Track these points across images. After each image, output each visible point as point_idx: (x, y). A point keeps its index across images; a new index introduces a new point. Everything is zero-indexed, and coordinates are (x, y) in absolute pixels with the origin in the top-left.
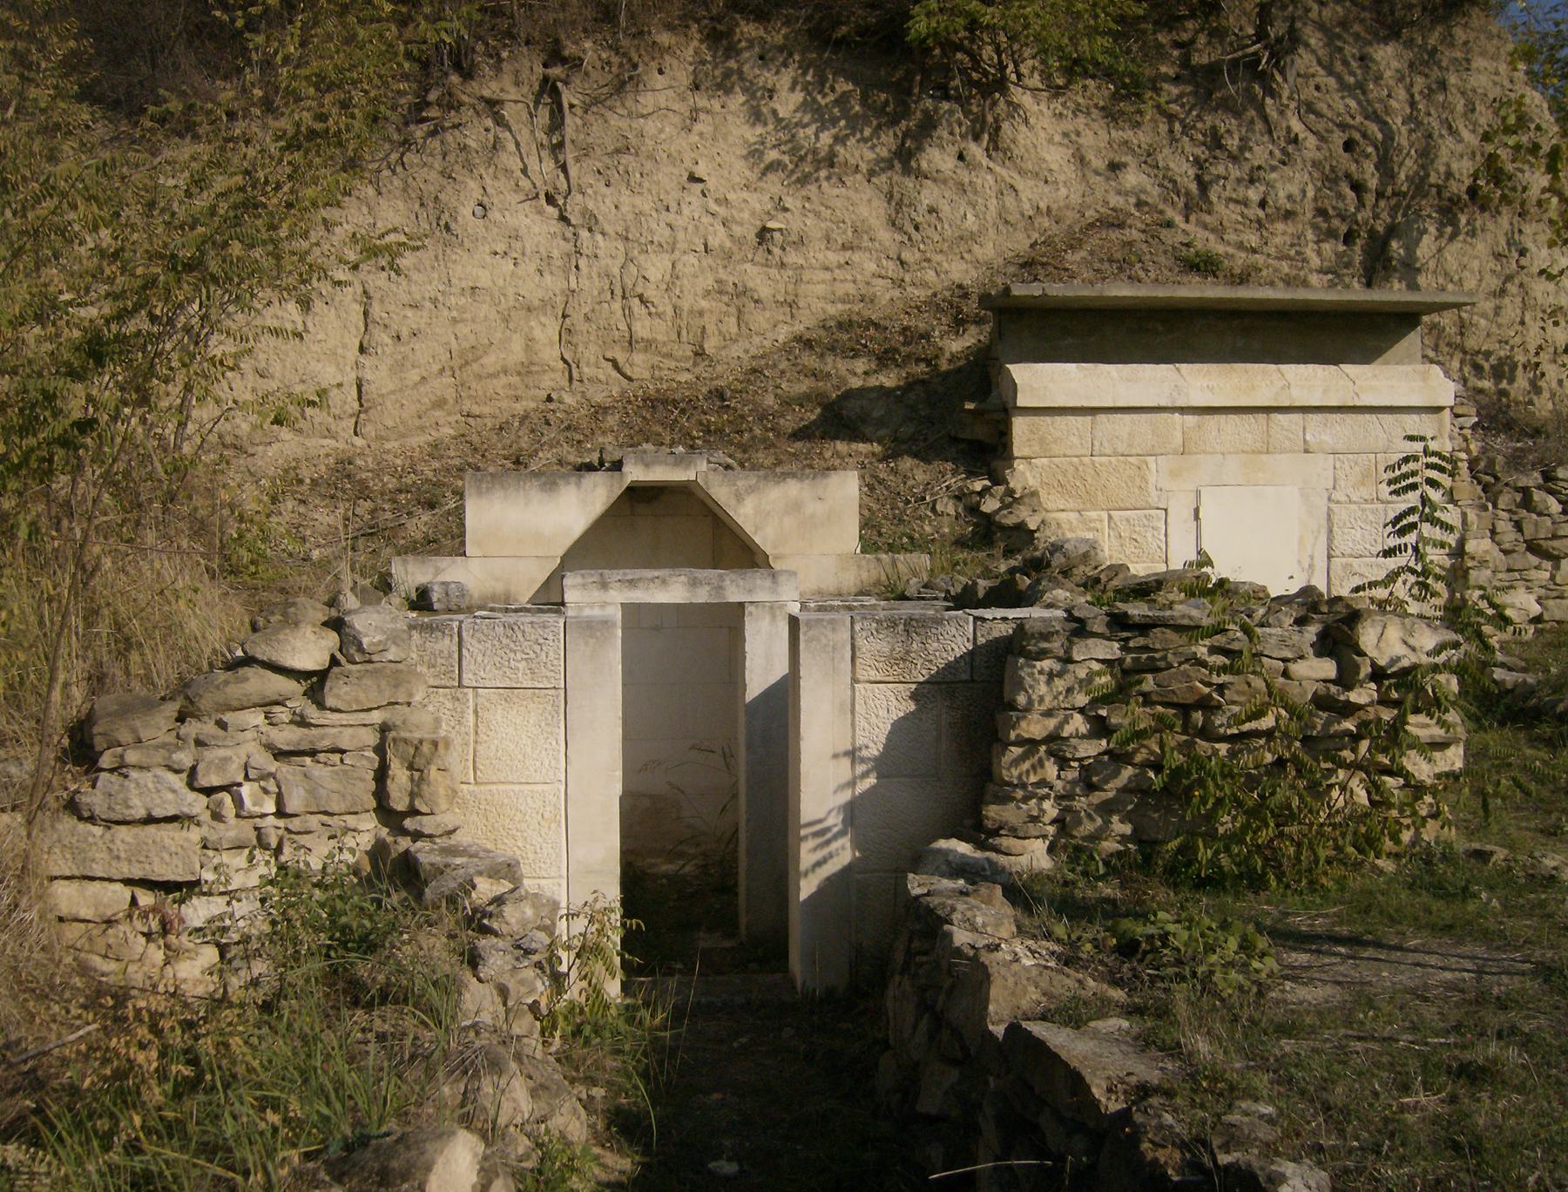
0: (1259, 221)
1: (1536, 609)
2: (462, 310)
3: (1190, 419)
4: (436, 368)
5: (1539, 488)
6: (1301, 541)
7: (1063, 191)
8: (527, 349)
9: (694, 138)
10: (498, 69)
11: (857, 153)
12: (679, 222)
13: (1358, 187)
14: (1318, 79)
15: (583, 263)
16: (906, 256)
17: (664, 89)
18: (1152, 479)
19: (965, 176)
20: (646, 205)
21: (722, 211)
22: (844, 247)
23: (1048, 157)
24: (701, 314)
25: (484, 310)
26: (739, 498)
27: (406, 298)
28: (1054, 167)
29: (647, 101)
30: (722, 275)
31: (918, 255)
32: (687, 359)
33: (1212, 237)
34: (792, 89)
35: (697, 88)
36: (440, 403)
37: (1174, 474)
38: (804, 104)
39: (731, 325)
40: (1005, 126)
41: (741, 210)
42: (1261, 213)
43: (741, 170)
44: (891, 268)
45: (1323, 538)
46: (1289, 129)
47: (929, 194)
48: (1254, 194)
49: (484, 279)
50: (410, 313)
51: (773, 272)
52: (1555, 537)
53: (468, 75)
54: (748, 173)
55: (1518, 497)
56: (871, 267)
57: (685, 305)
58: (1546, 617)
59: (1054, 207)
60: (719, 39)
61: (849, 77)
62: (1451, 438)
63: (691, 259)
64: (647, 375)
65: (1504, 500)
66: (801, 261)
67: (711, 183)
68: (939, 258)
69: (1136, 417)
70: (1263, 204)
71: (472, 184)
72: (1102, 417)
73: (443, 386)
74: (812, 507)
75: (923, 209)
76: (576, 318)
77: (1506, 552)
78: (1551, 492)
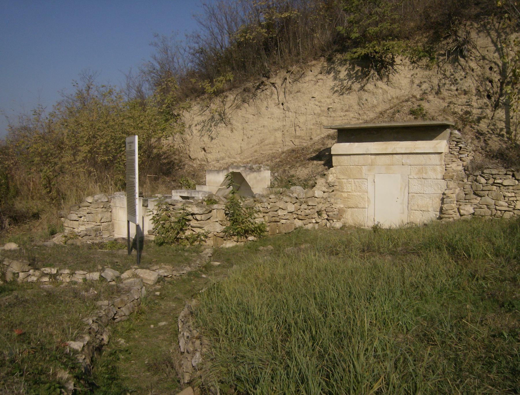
0: (456, 95)
1: (472, 211)
2: (261, 131)
3: (373, 157)
4: (256, 143)
5: (480, 175)
6: (401, 188)
7: (403, 91)
8: (275, 139)
9: (317, 86)
10: (276, 75)
11: (356, 86)
12: (308, 107)
13: (491, 82)
14: (488, 48)
15: (286, 119)
16: (360, 112)
17: (310, 76)
18: (364, 171)
19: (375, 90)
20: (300, 104)
21: (319, 104)
22: (346, 111)
23: (402, 82)
24: (311, 129)
25: (266, 131)
26: (247, 176)
27: (250, 129)
28: (403, 85)
29: (307, 79)
30: (317, 120)
31: (363, 112)
32: (308, 140)
33: (441, 101)
34: (346, 71)
35: (321, 73)
36: (256, 151)
37: (369, 170)
38: (347, 74)
39: (318, 132)
40: (390, 75)
41: (324, 104)
42: (456, 93)
43: (327, 92)
44: (357, 115)
45: (407, 188)
46: (469, 67)
47: (365, 96)
48: (454, 88)
49: (266, 123)
50: (251, 132)
51: (329, 118)
52: (482, 190)
53: (268, 78)
54: (329, 94)
55: (475, 178)
56: (352, 115)
57: (308, 128)
58: (476, 214)
59: (399, 96)
60: (330, 60)
61: (358, 65)
62: (444, 161)
63: (310, 116)
64: (298, 144)
65: (471, 178)
66: (334, 115)
67: (317, 98)
68: (367, 112)
69: (360, 156)
70: (457, 90)
71: (265, 103)
72: (352, 156)
73: (257, 147)
74: (258, 178)
75: (364, 99)
76: (285, 131)
77: (466, 194)
78: (484, 177)
